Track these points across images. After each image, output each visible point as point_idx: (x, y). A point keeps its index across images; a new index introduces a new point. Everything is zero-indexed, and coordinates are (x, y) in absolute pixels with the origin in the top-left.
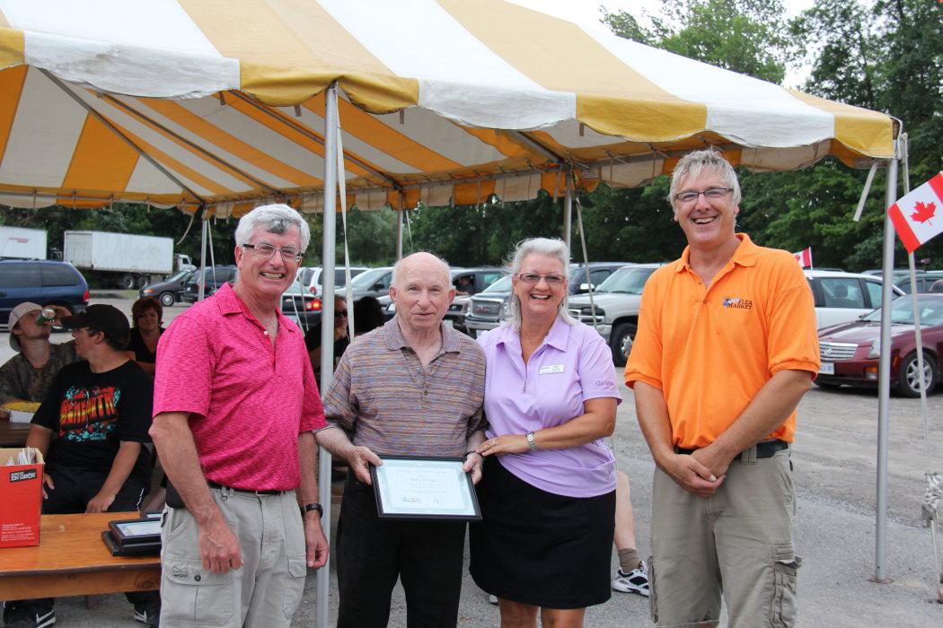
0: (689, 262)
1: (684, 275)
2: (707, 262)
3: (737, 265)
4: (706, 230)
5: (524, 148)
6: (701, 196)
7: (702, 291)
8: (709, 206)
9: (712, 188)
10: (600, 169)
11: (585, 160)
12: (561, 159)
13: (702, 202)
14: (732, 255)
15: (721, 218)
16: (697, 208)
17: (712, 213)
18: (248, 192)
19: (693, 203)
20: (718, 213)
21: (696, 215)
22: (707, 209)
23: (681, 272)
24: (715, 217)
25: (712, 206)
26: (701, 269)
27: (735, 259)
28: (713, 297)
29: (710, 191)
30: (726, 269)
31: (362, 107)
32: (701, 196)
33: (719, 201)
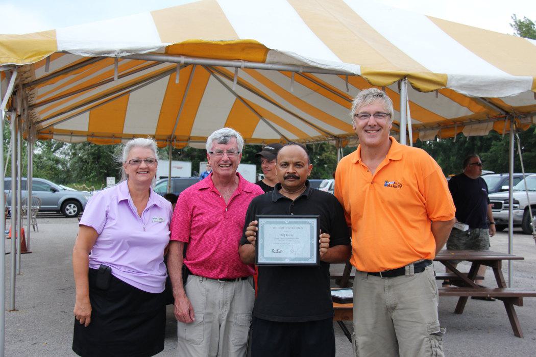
0: (360, 156)
1: (358, 165)
2: (372, 157)
3: (391, 160)
4: (373, 137)
5: (485, 107)
6: (372, 117)
7: (370, 176)
8: (376, 123)
9: (379, 112)
10: (532, 117)
11: (523, 113)
12: (507, 113)
13: (372, 120)
14: (387, 152)
15: (382, 130)
16: (369, 124)
17: (377, 128)
18: (318, 137)
19: (366, 121)
20: (380, 128)
21: (368, 128)
22: (375, 125)
23: (355, 163)
24: (378, 130)
25: (378, 123)
26: (368, 163)
27: (390, 157)
28: (377, 180)
29: (377, 114)
30: (384, 162)
31: (418, 89)
32: (372, 117)
33: (382, 121)
